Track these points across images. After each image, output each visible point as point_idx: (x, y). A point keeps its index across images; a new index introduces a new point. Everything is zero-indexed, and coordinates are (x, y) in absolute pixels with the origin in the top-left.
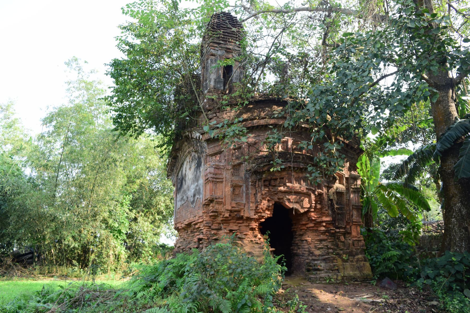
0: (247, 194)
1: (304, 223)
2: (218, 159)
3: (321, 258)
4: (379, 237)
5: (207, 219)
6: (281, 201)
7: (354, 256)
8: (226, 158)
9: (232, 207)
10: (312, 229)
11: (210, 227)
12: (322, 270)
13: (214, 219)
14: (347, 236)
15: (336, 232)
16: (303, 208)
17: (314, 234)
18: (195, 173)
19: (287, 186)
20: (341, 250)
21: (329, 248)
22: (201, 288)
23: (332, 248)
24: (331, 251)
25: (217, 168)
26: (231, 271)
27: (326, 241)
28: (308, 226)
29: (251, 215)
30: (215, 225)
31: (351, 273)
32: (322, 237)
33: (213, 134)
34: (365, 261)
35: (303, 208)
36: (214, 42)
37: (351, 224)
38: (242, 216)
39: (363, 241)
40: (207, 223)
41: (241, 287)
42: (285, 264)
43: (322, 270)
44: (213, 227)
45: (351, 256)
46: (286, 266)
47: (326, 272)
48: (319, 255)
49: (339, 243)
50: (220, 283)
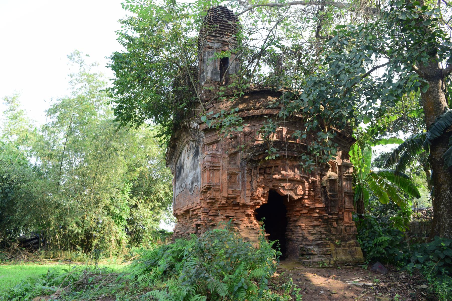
0: (243, 182)
1: (298, 209)
2: (215, 148)
4: (370, 223)
5: (205, 205)
6: (276, 188)
7: (346, 241)
8: (223, 147)
9: (229, 194)
10: (305, 215)
11: (207, 213)
13: (211, 205)
15: (328, 218)
16: (296, 195)
17: (308, 220)
18: (193, 161)
19: (281, 174)
20: (334, 235)
21: (322, 234)
22: (199, 271)
23: (325, 234)
24: (324, 236)
25: (214, 156)
26: (227, 255)
28: (302, 212)
29: (247, 202)
30: (213, 211)
31: (344, 258)
32: (315, 223)
33: (210, 124)
34: (357, 246)
35: (296, 195)
36: (211, 36)
37: (343, 211)
38: (239, 203)
39: (355, 227)
40: (204, 210)
41: (237, 271)
42: (279, 249)
44: (210, 213)
45: (344, 241)
46: (280, 251)
47: (320, 257)
48: (313, 241)
49: (332, 229)
50: (218, 267)
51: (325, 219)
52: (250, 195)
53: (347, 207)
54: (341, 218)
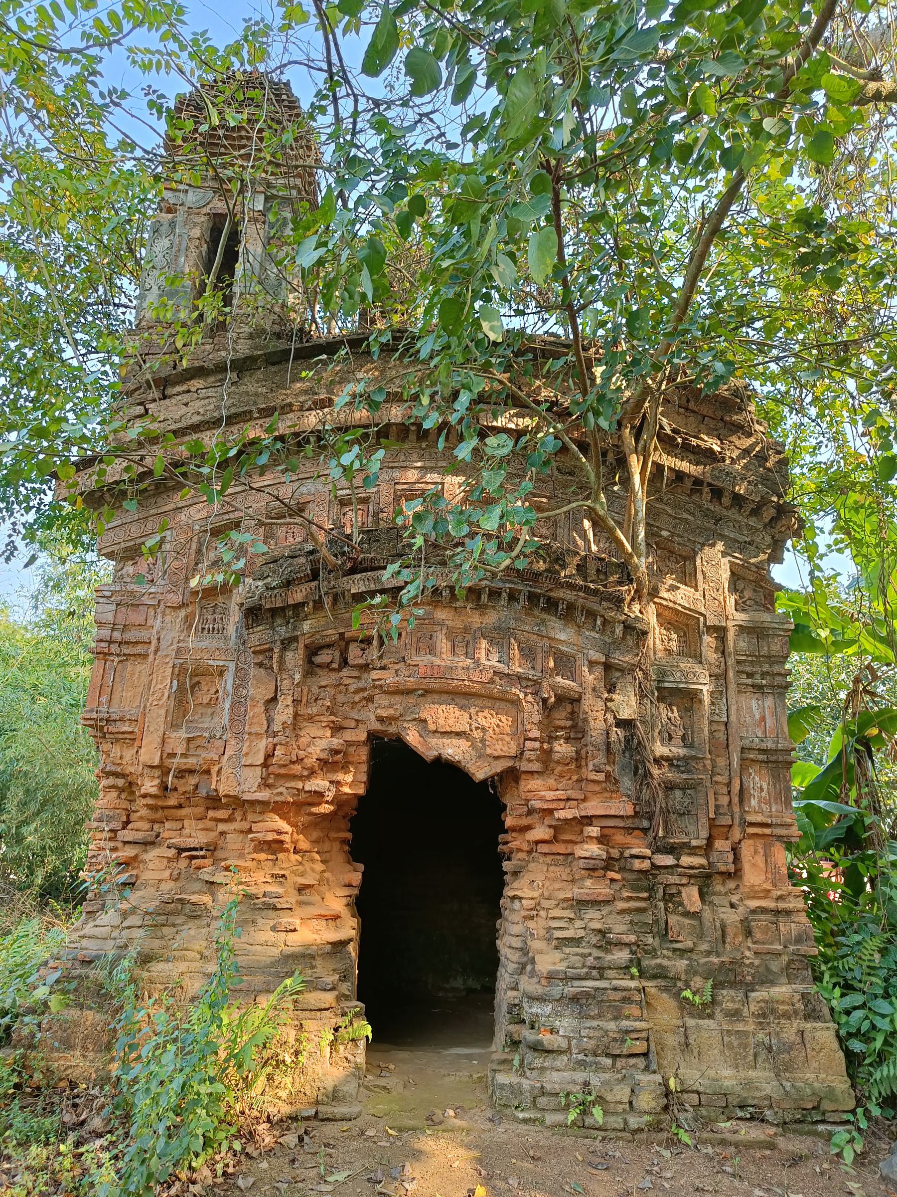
6: (392, 729)
7: (750, 988)
12: (560, 1052)
15: (653, 865)
23: (627, 945)
24: (622, 956)
27: (606, 910)
29: (245, 787)
31: (728, 1077)
34: (812, 1015)
37: (736, 834)
39: (803, 918)
43: (560, 1052)
45: (733, 985)
49: (673, 920)
53: (759, 818)
54: (723, 868)
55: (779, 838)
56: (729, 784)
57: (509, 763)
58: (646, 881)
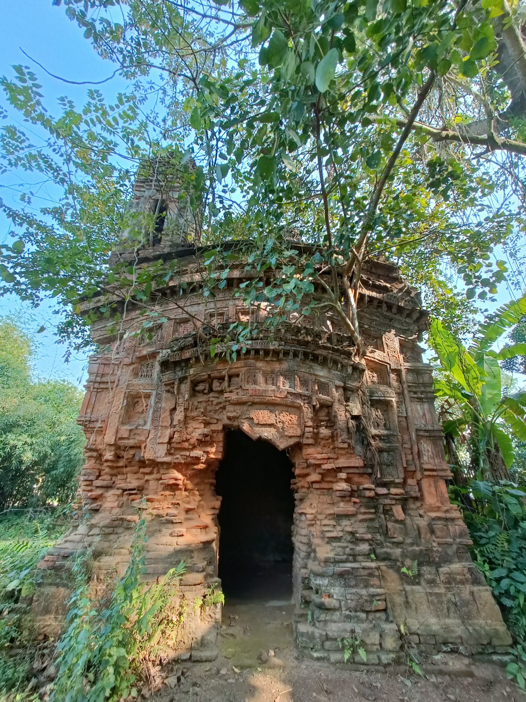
3: (331, 569)
4: (507, 510)
6: (235, 424)
7: (438, 566)
12: (334, 610)
14: (412, 506)
15: (377, 494)
20: (398, 544)
21: (356, 540)
23: (367, 540)
24: (364, 547)
27: (353, 520)
29: (158, 455)
31: (434, 623)
32: (343, 507)
34: (476, 582)
37: (419, 475)
39: (461, 522)
43: (334, 610)
45: (429, 563)
47: (348, 618)
48: (327, 561)
49: (390, 525)
51: (369, 497)
52: (166, 440)
54: (414, 495)
55: (441, 477)
56: (411, 449)
57: (296, 440)
58: (373, 502)
